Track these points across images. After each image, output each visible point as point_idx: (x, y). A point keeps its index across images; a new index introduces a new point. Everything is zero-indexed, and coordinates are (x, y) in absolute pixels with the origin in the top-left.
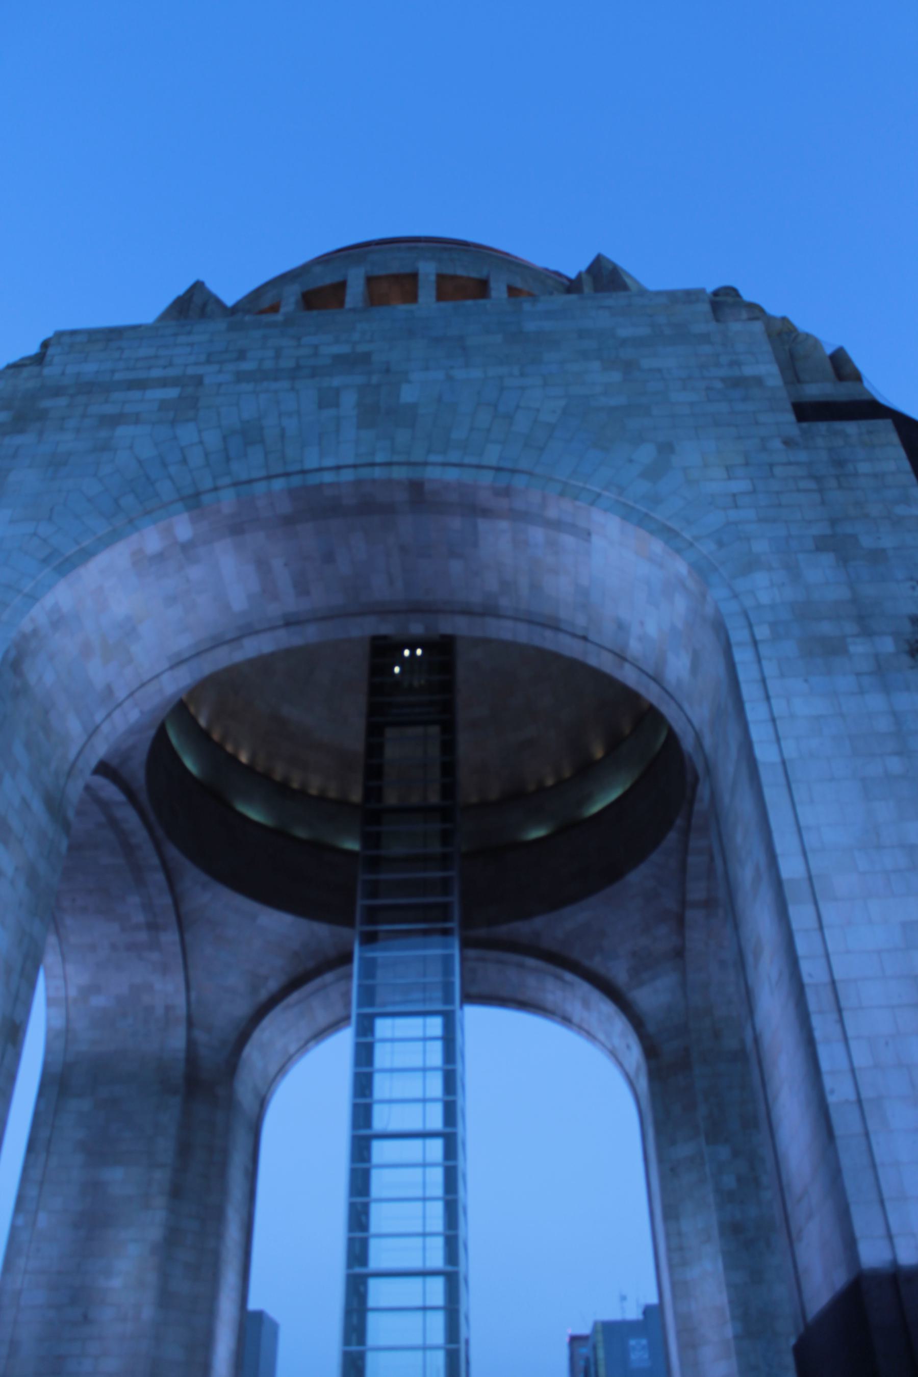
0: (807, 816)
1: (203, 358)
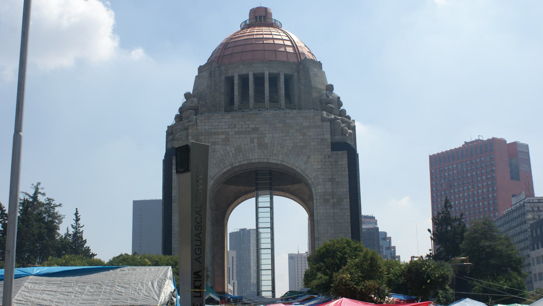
1: (228, 127)
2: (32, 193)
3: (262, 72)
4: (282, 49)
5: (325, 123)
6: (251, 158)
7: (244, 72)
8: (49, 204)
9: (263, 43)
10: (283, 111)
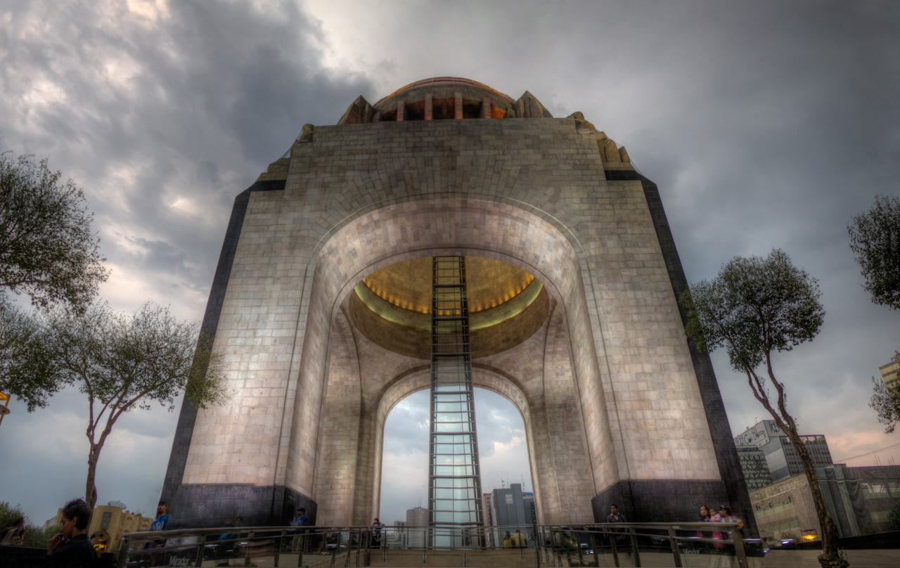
0: (606, 335)
6: (425, 192)
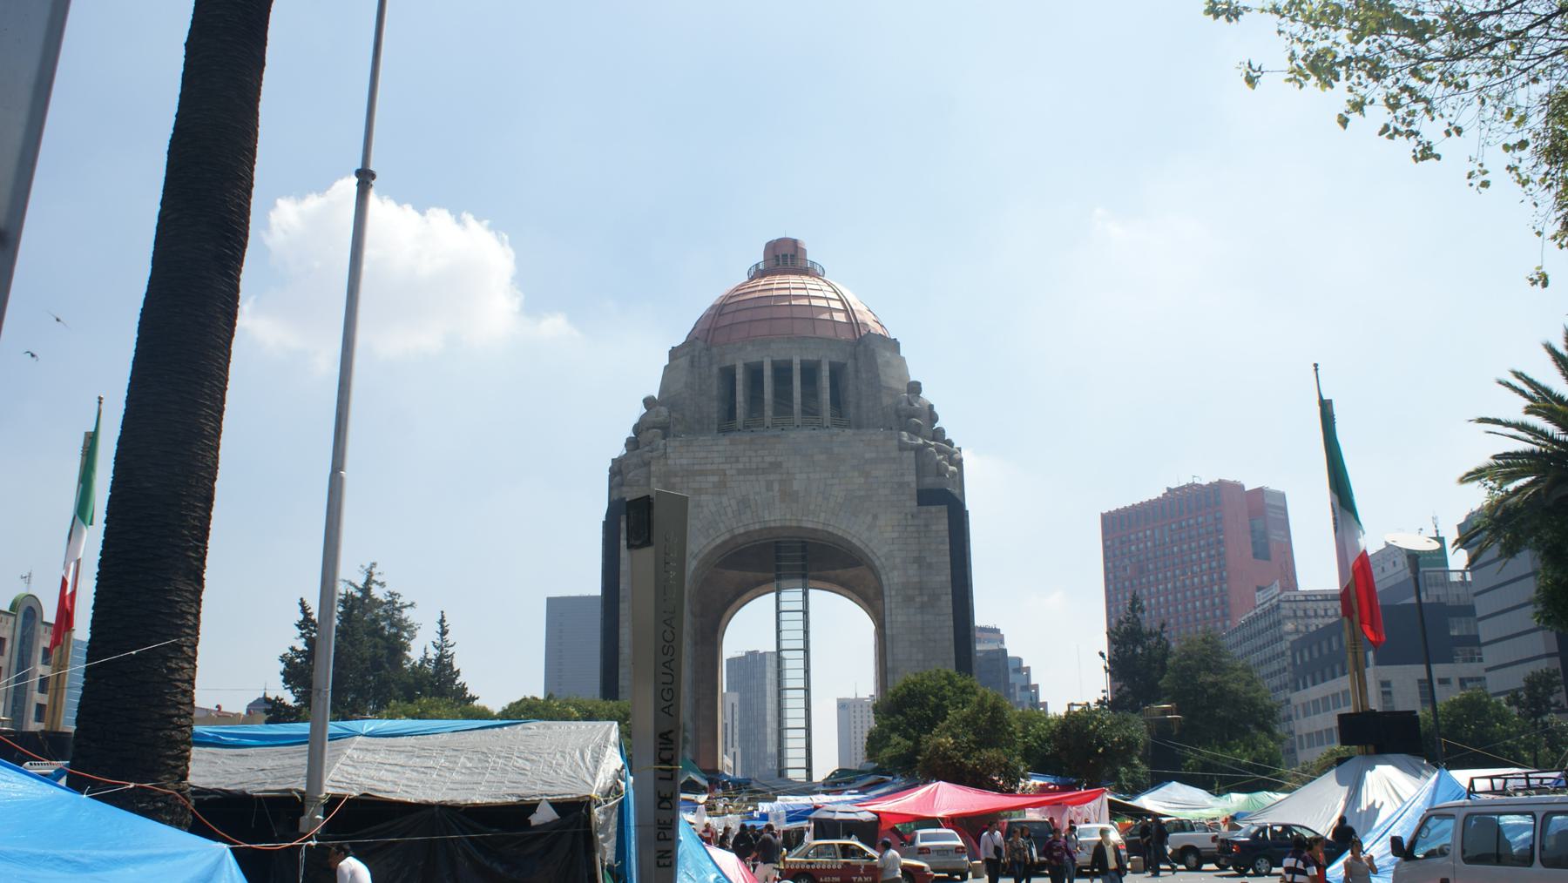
2: (360, 582)
3: (787, 358)
4: (826, 316)
5: (906, 454)
7: (754, 358)
8: (392, 603)
9: (790, 305)
10: (827, 430)
